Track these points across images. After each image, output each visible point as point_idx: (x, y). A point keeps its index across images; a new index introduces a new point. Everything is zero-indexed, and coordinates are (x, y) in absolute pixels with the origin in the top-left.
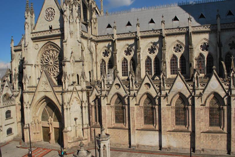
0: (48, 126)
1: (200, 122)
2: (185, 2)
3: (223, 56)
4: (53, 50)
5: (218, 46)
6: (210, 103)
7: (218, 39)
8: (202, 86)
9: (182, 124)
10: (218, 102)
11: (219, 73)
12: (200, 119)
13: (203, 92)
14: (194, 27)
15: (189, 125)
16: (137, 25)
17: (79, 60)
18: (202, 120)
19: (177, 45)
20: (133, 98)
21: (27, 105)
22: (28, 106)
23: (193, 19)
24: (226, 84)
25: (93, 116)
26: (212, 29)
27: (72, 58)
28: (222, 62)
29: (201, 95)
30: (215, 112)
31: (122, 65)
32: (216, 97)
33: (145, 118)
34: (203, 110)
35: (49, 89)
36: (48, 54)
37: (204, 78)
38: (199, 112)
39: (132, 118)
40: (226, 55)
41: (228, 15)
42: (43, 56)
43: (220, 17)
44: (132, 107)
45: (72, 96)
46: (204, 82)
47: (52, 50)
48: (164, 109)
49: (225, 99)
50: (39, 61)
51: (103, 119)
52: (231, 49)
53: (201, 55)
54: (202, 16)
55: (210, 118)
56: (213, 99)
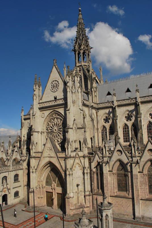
0: (51, 191)
4: (57, 118)
16: (136, 91)
17: (81, 127)
20: (136, 165)
21: (33, 170)
22: (34, 171)
25: (95, 183)
27: (75, 126)
31: (123, 131)
35: (53, 154)
36: (53, 122)
39: (136, 187)
42: (48, 124)
44: (135, 175)
45: (75, 162)
47: (56, 118)
50: (45, 128)
51: (106, 186)
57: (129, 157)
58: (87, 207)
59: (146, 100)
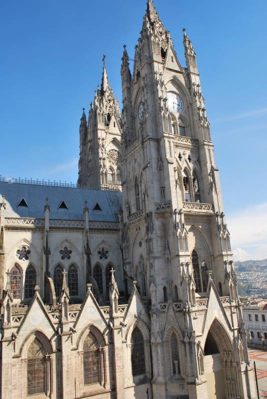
1: (11, 391)
3: (51, 270)
5: (45, 254)
6: (29, 351)
7: (45, 242)
8: (16, 321)
9: (95, 382)
10: (96, 341)
11: (45, 295)
12: (11, 384)
13: (18, 332)
14: (8, 218)
15: (105, 381)
18: (14, 386)
20: (9, 344)
23: (8, 205)
24: (55, 314)
26: (37, 225)
28: (49, 278)
29: (14, 338)
30: (36, 367)
32: (39, 338)
34: (18, 366)
37: (20, 306)
38: (9, 370)
40: (56, 268)
41: (60, 207)
43: (49, 209)
46: (19, 313)
49: (53, 341)
52: (63, 258)
53: (17, 266)
54: (23, 203)
55: (28, 378)
56: (34, 344)
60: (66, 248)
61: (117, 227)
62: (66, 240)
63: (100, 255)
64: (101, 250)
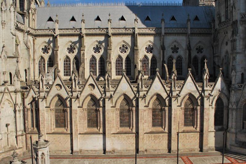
1: (143, 123)
2: (163, 3)
3: (166, 60)
5: (162, 50)
6: (153, 104)
7: (162, 43)
8: (146, 87)
9: (190, 125)
10: (192, 103)
11: (162, 74)
12: (143, 120)
13: (147, 93)
14: (140, 28)
15: (197, 126)
16: (108, 21)
17: (13, 56)
18: (145, 121)
19: (123, 46)
23: (139, 20)
24: (168, 86)
26: (157, 32)
27: (4, 53)
28: (165, 64)
29: (145, 97)
30: (157, 113)
31: (64, 64)
32: (159, 98)
33: (89, 121)
34: (147, 111)
37: (148, 80)
38: (143, 113)
39: (74, 122)
40: (169, 59)
43: (164, 21)
44: (74, 110)
45: (3, 98)
46: (147, 84)
48: (108, 111)
49: (166, 100)
52: (173, 52)
54: (148, 19)
55: (153, 118)
57: (135, 91)
58: (19, 148)
59: (118, 32)
60: (175, 46)
61: (210, 31)
62: (175, 41)
63: (197, 51)
64: (198, 47)
